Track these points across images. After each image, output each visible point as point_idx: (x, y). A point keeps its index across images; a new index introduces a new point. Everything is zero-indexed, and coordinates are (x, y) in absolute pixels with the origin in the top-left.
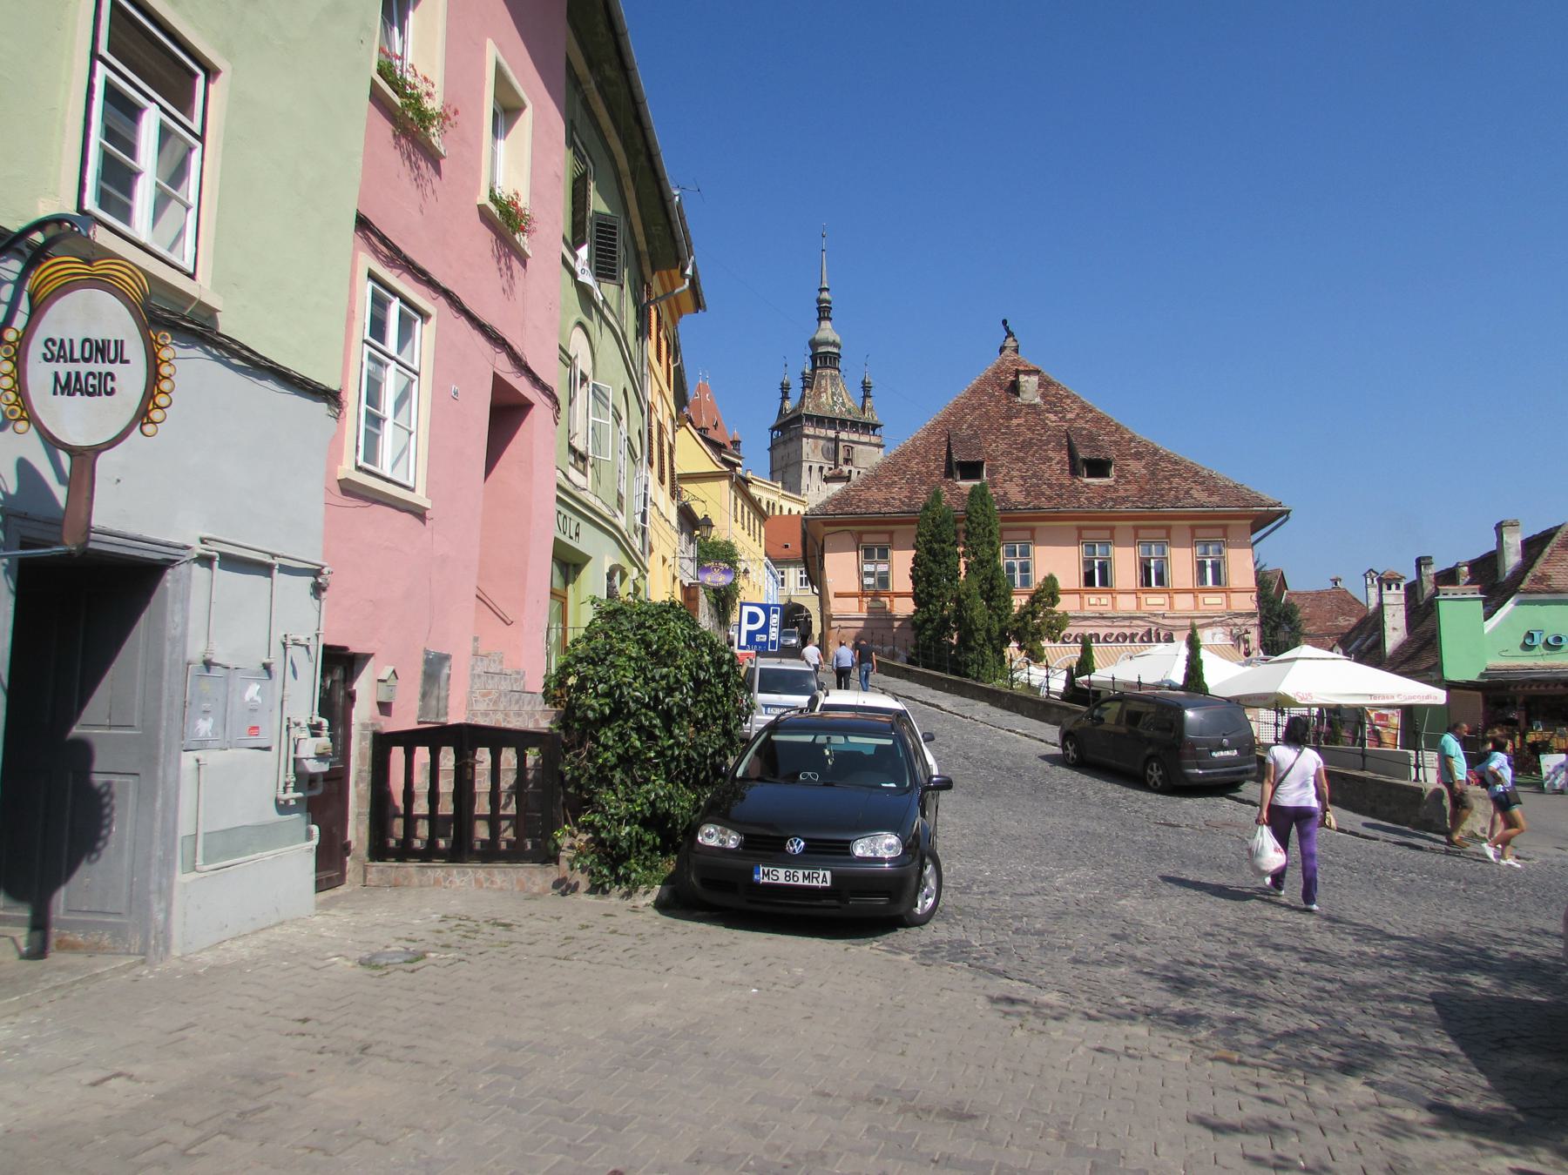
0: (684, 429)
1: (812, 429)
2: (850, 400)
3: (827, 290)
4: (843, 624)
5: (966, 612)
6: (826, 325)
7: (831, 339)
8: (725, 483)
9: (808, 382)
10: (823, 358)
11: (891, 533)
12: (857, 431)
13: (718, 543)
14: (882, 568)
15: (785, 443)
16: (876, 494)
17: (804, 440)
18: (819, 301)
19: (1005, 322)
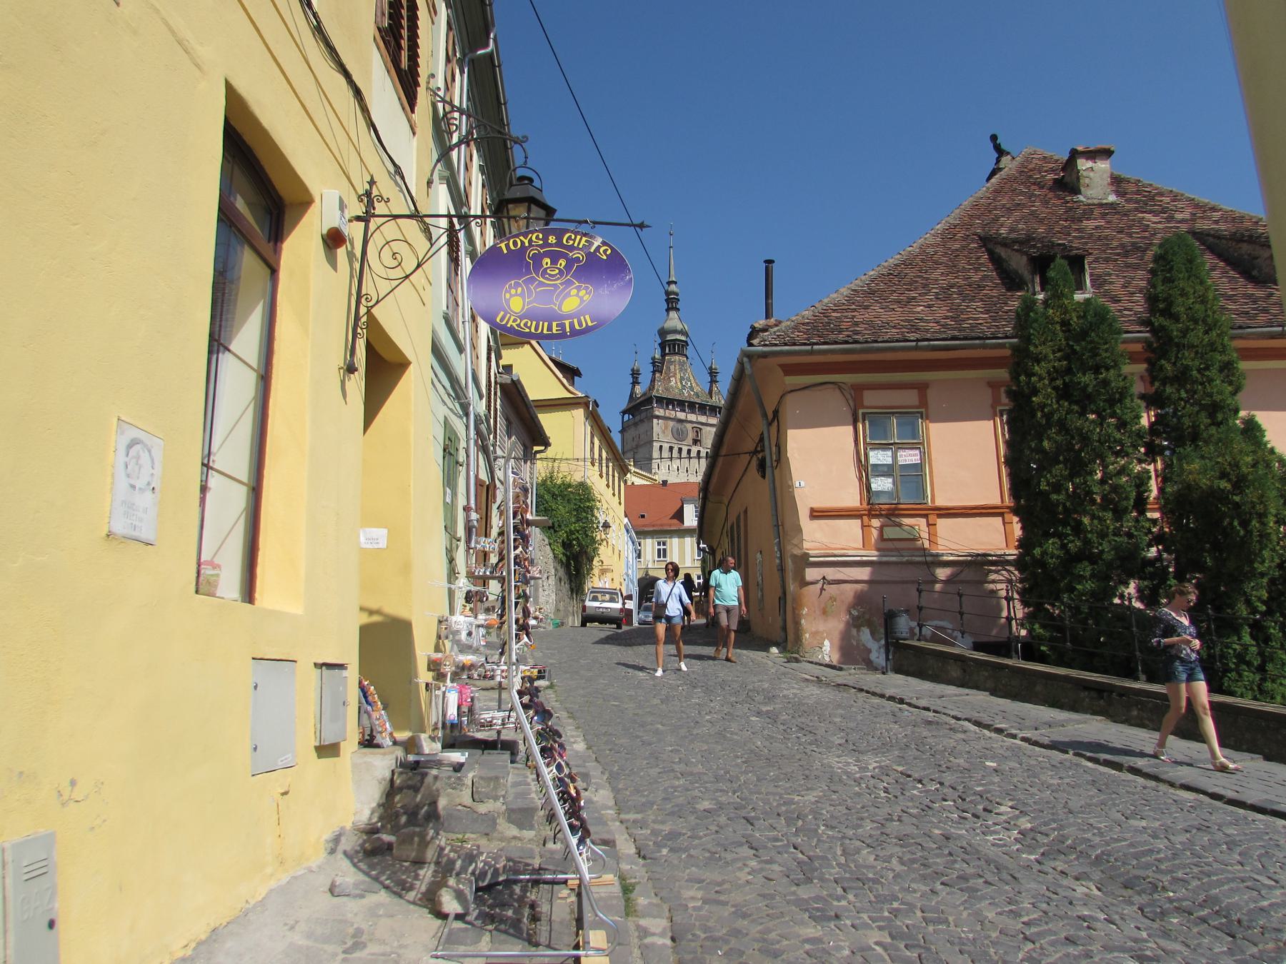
0: (527, 347)
1: (662, 411)
2: (698, 385)
3: (675, 283)
4: (831, 573)
5: (1245, 524)
6: (673, 314)
7: (679, 327)
8: (579, 413)
9: (657, 367)
10: (671, 346)
11: (922, 388)
12: (705, 414)
13: (570, 485)
14: (909, 457)
15: (636, 424)
16: (877, 313)
17: (655, 421)
18: (667, 293)
19: (994, 138)
